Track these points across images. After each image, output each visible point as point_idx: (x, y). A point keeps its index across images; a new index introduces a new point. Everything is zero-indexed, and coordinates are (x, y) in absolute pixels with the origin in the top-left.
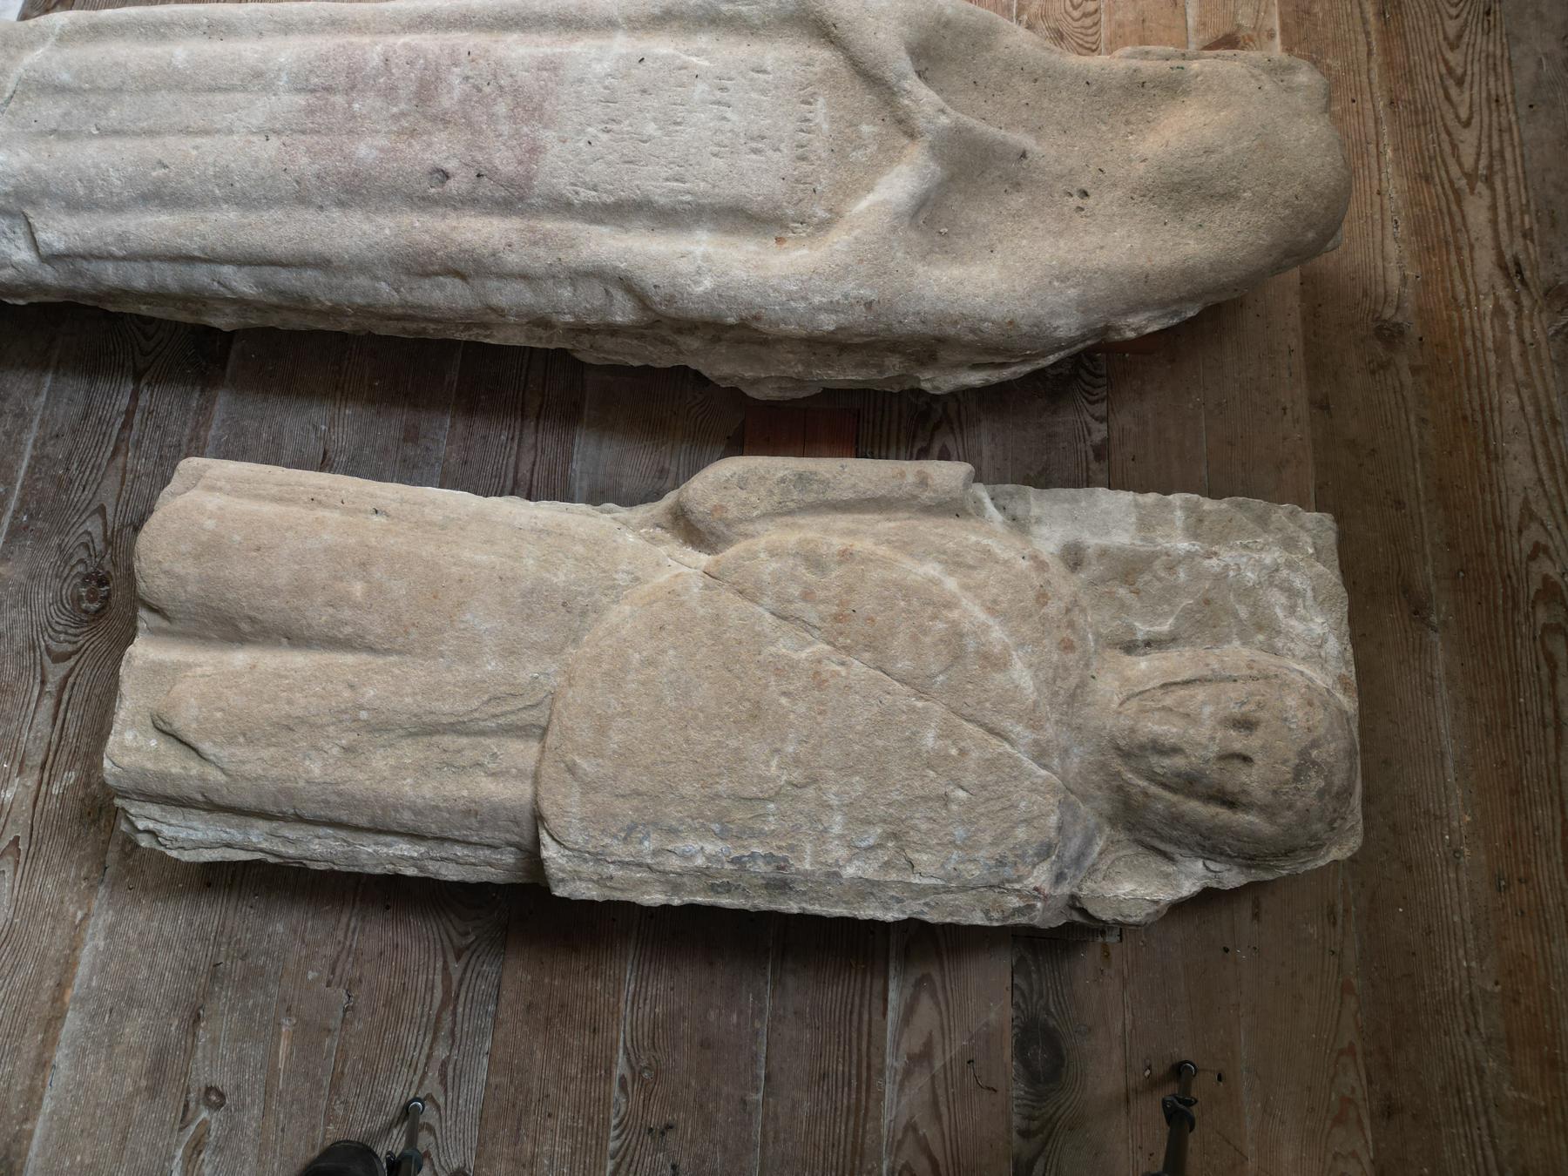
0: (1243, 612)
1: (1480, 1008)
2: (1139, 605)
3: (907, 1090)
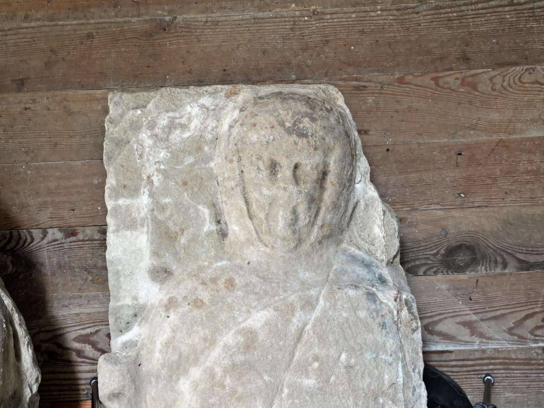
0: (190, 160)
1: (403, 5)
2: (191, 229)
3: (491, 335)
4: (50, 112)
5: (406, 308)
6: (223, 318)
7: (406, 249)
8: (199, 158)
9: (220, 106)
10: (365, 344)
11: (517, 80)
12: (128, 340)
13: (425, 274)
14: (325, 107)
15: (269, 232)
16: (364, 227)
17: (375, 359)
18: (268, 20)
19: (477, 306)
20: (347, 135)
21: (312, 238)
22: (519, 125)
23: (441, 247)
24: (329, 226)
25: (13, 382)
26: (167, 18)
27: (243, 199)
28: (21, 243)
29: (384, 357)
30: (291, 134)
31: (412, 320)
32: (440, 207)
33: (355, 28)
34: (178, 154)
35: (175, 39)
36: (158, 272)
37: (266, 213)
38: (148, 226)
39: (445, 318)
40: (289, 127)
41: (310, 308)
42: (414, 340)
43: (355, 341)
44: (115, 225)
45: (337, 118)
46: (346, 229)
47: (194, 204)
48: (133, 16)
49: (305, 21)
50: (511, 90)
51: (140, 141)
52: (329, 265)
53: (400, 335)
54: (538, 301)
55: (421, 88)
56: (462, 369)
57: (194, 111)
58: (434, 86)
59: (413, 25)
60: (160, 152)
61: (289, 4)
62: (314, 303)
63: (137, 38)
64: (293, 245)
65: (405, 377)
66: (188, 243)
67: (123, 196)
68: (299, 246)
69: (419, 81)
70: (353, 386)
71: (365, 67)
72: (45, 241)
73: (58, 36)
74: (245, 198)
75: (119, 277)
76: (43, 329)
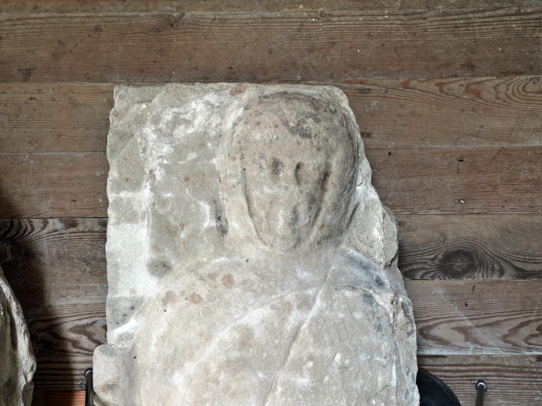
0: (192, 156)
1: (411, 10)
2: (192, 224)
3: (485, 342)
4: (55, 102)
5: (402, 311)
6: (220, 314)
7: (404, 253)
8: (202, 154)
9: (225, 103)
10: (360, 345)
11: (520, 89)
12: (124, 332)
13: (422, 278)
14: (329, 108)
15: (270, 230)
16: (363, 229)
17: (369, 361)
18: (275, 20)
19: (473, 312)
20: (350, 137)
21: (312, 237)
22: (521, 134)
23: (439, 252)
24: (329, 226)
25: (9, 370)
26: (176, 15)
27: (245, 197)
28: (21, 232)
29: (378, 359)
30: (295, 134)
31: (407, 323)
32: (439, 212)
33: (362, 31)
34: (181, 150)
35: (182, 35)
36: (157, 266)
37: (266, 212)
38: (148, 219)
39: (441, 323)
40: (293, 127)
41: (307, 307)
42: (409, 343)
43: (350, 342)
44: (116, 218)
45: (341, 120)
46: (346, 230)
47: (195, 199)
48: (142, 12)
49: (312, 22)
50: (514, 98)
51: (144, 135)
52: (328, 266)
53: (396, 338)
54: (534, 310)
55: (425, 93)
56: (455, 375)
57: (199, 108)
58: (438, 92)
59: (419, 31)
60: (164, 147)
61: (297, 5)
62: (311, 303)
63: (144, 33)
64: (292, 244)
65: (398, 379)
66: (188, 238)
67: (125, 189)
68: (298, 245)
69: (423, 86)
70: (347, 386)
71: (370, 71)
72: (45, 231)
73: (66, 28)
74: (246, 195)
75: (118, 270)
76: (40, 318)
